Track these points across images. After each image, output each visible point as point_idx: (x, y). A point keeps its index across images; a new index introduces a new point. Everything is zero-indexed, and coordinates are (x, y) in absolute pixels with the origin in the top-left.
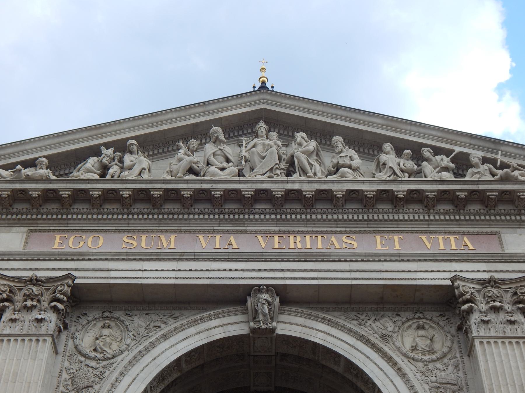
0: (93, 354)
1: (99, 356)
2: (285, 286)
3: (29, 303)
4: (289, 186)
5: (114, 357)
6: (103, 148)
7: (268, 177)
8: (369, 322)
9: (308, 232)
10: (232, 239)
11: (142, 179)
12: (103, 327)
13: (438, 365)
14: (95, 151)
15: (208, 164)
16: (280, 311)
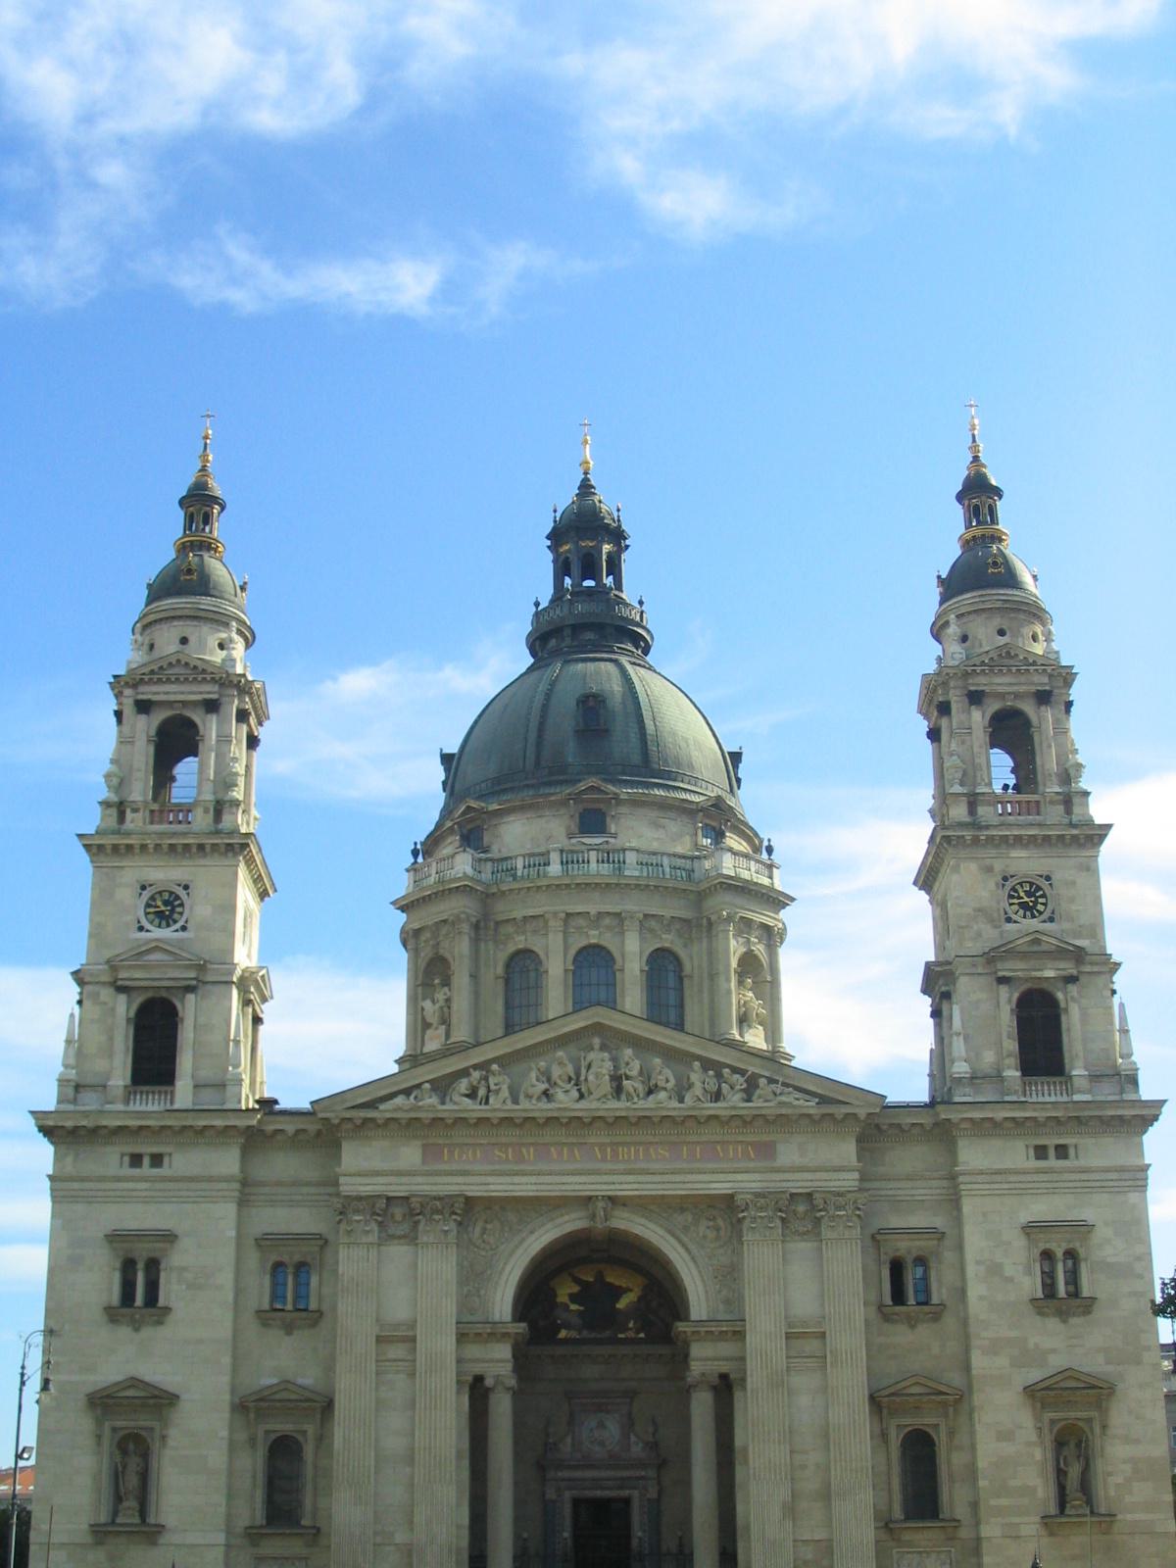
0: (483, 1245)
1: (488, 1247)
2: (616, 1196)
3: (437, 1217)
4: (618, 1114)
5: (497, 1247)
6: (471, 1070)
7: (604, 1102)
8: (675, 1215)
9: (636, 1144)
10: (576, 1151)
11: (505, 1107)
12: (486, 1222)
13: (721, 1251)
14: (464, 1073)
15: (555, 1083)
16: (612, 1209)
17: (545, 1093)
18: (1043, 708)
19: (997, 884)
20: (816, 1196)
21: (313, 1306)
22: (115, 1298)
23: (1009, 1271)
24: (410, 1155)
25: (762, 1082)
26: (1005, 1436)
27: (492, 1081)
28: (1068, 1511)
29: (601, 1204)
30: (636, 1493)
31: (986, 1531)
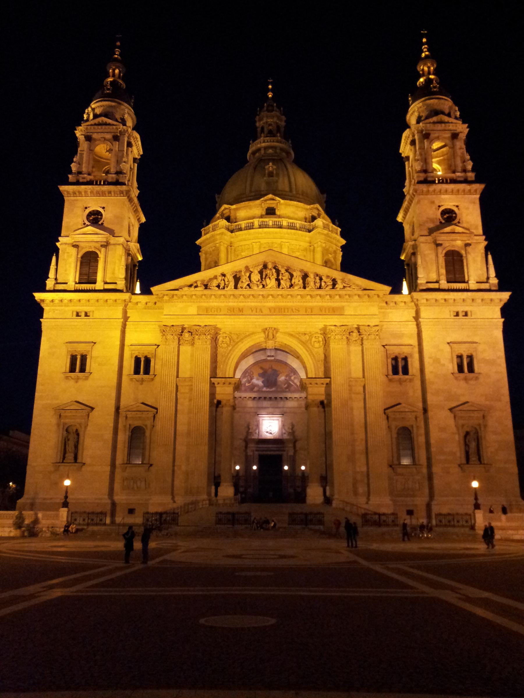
14: (215, 277)
17: (248, 285)
18: (455, 140)
19: (436, 209)
20: (361, 328)
21: (152, 372)
22: (68, 370)
23: (442, 363)
24: (192, 310)
25: (339, 282)
26: (443, 429)
27: (226, 280)
28: (470, 463)
29: (271, 331)
30: (285, 453)
31: (435, 469)
